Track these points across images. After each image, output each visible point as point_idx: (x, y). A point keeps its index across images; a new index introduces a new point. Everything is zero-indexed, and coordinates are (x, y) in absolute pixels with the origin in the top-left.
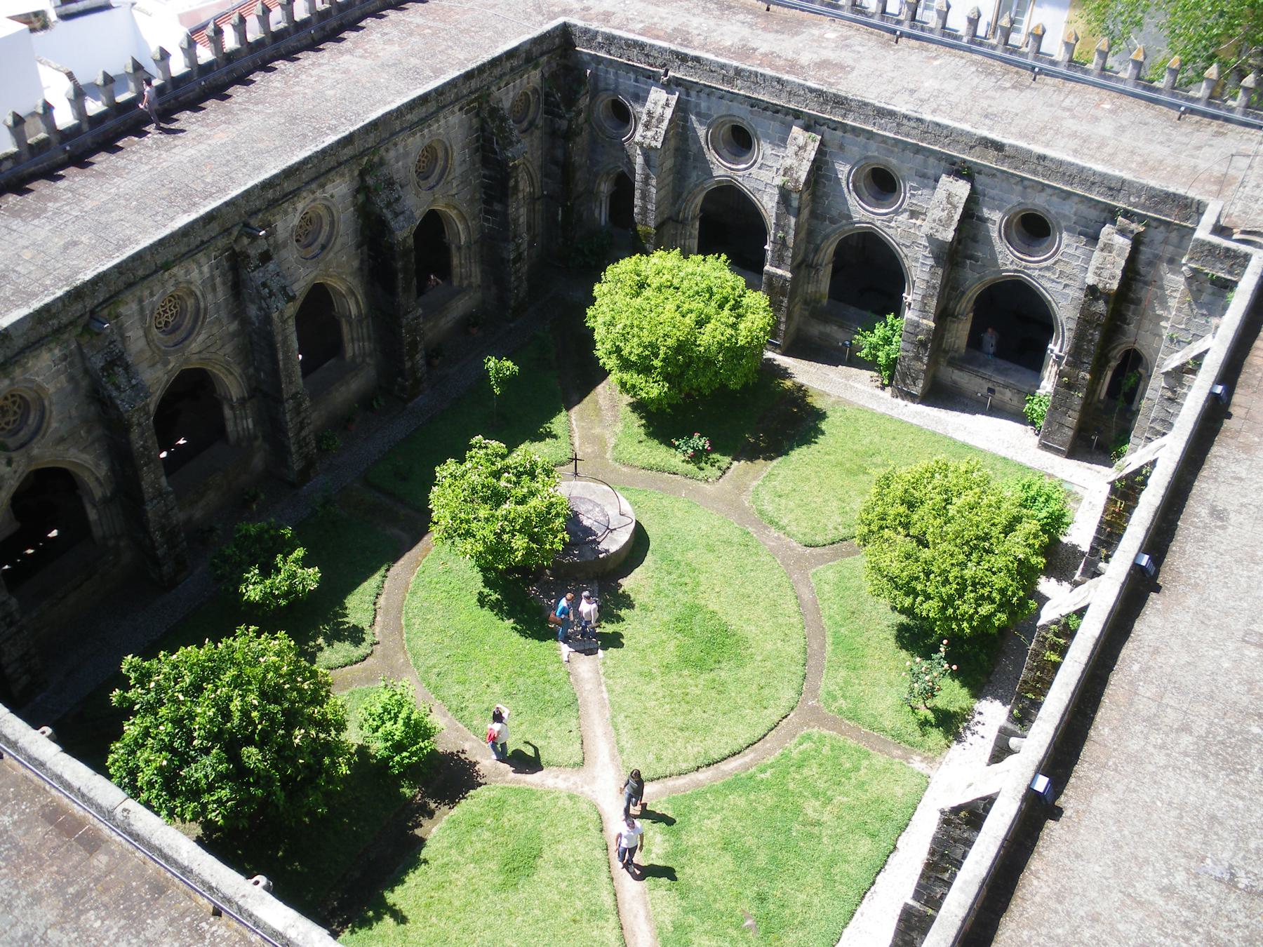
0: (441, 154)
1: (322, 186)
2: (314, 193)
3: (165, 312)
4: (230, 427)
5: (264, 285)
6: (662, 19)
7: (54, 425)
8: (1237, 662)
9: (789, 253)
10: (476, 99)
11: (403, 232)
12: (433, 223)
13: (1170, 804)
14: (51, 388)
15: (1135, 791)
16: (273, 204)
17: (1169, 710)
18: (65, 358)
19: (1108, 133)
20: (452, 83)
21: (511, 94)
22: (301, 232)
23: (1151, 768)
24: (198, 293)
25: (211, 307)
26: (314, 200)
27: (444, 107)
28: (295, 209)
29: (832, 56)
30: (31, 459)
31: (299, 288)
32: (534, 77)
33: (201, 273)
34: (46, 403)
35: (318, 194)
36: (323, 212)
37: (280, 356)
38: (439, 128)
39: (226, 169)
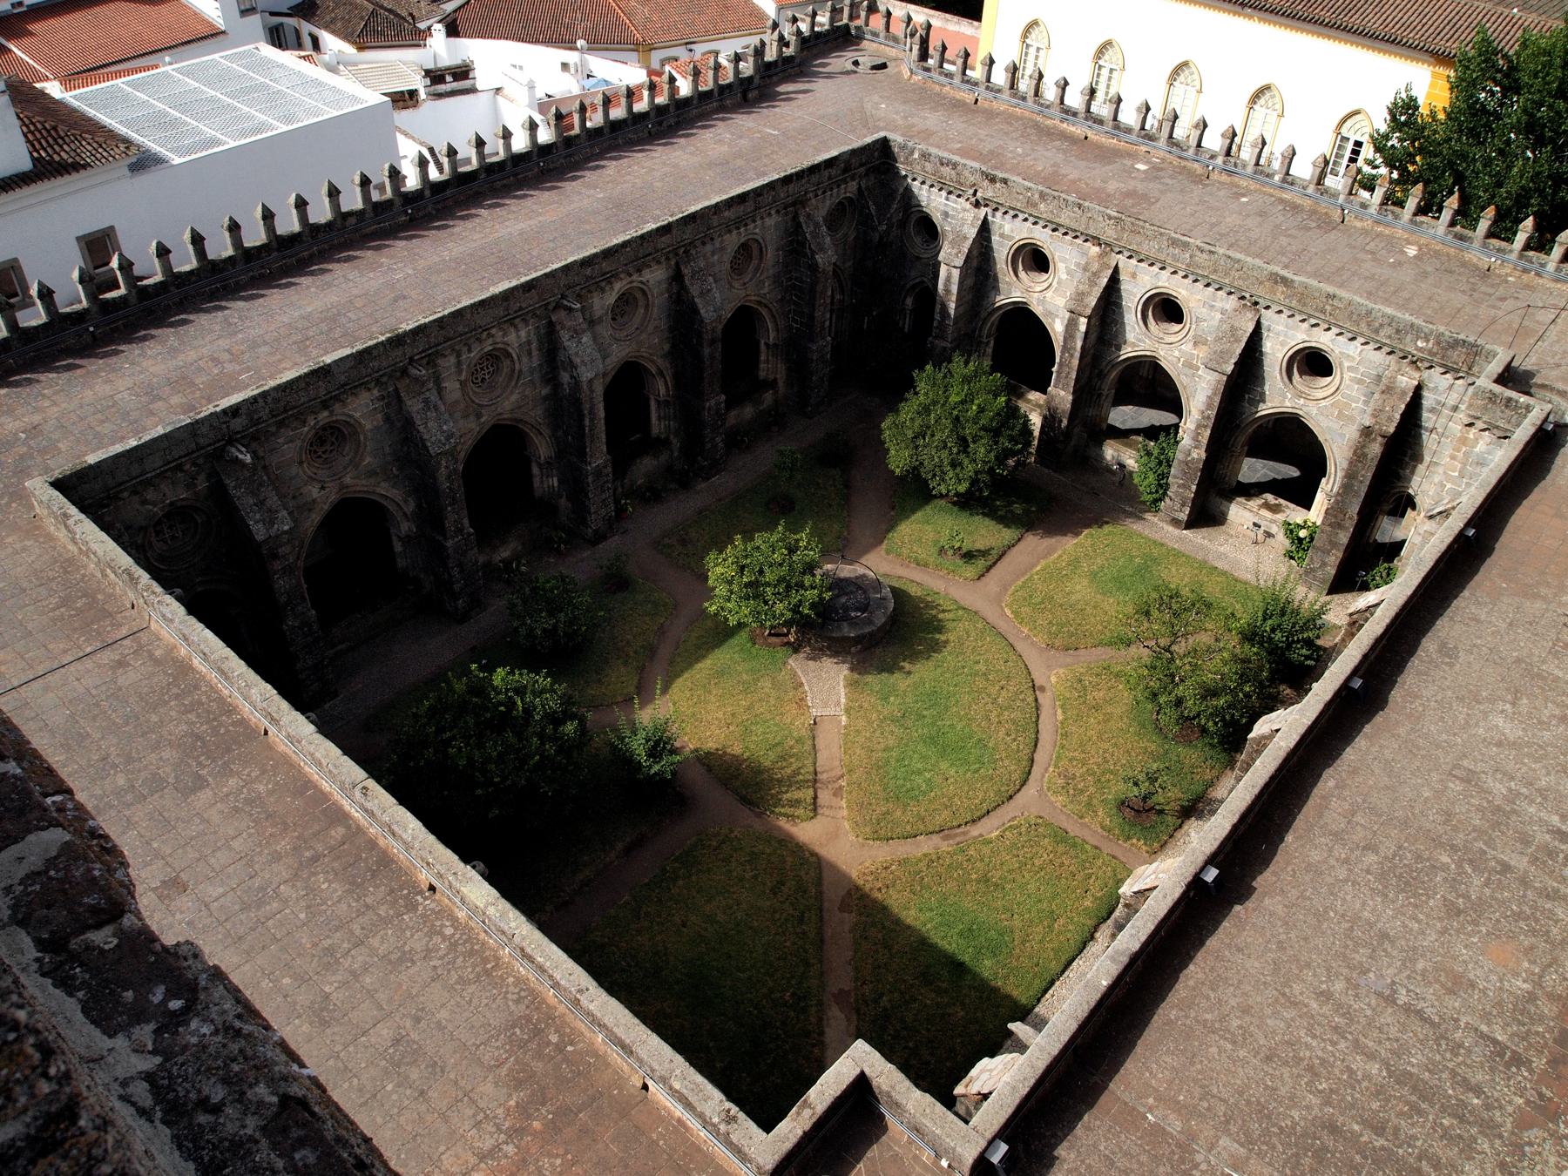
0: (755, 253)
1: (639, 271)
2: (630, 275)
3: (482, 369)
4: (536, 482)
6: (981, 140)
7: (368, 460)
8: (1439, 794)
12: (744, 320)
13: (1343, 916)
15: (1309, 899)
17: (1359, 828)
18: (382, 398)
20: (771, 186)
21: (828, 203)
22: (617, 311)
23: (1330, 880)
25: (525, 369)
28: (612, 288)
29: (1140, 187)
33: (518, 337)
35: (635, 277)
37: (587, 422)
38: (755, 227)
39: (551, 245)
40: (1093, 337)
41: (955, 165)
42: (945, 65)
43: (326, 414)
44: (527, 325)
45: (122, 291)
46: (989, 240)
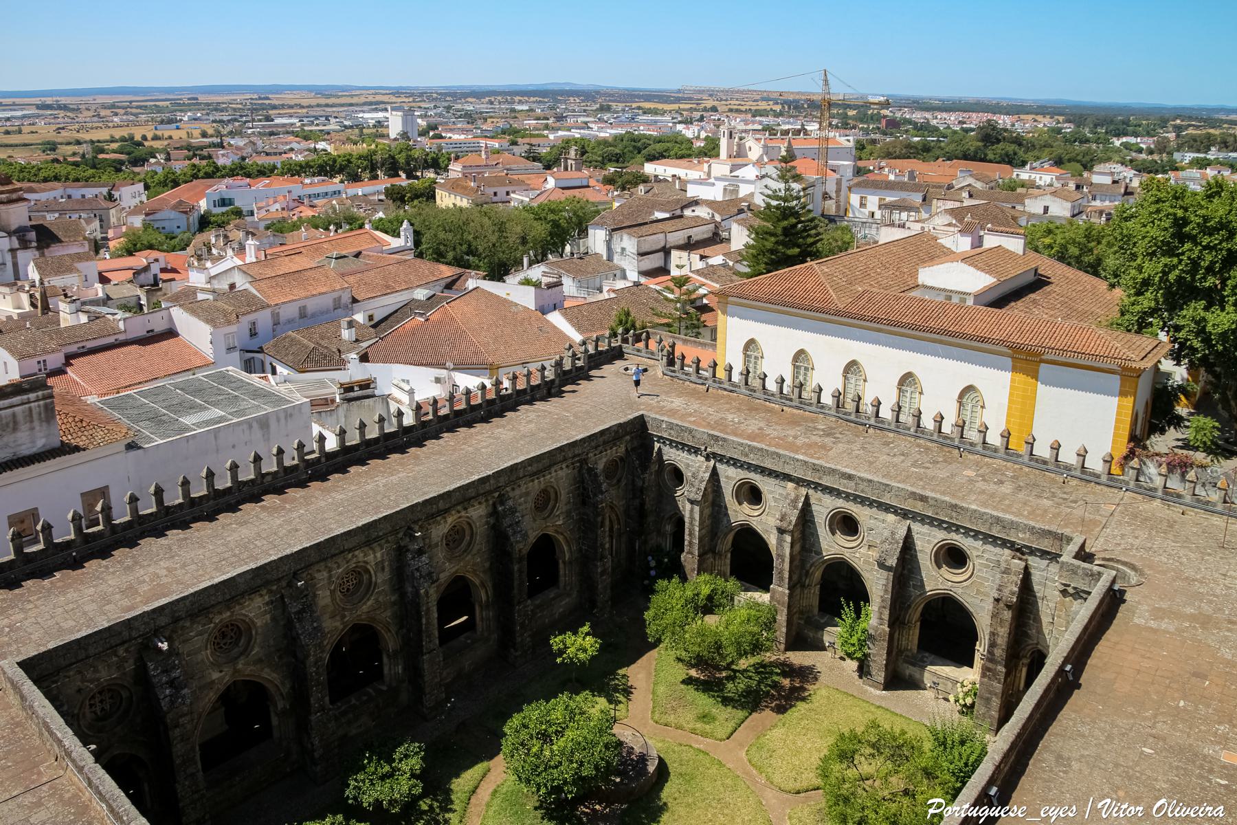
0: (553, 496)
1: (465, 509)
5: (417, 570)
7: (256, 650)
9: (786, 575)
10: (578, 461)
11: (521, 546)
12: (545, 545)
14: (259, 623)
16: (432, 516)
18: (272, 602)
19: (1008, 491)
21: (604, 460)
22: (450, 538)
24: (372, 572)
26: (460, 517)
27: (555, 464)
28: (446, 522)
30: (236, 671)
31: (444, 577)
32: (620, 450)
33: (375, 557)
34: (254, 632)
35: (463, 513)
36: (466, 527)
37: (424, 621)
40: (797, 547)
41: (691, 431)
42: (685, 368)
43: (228, 614)
44: (382, 549)
45: (101, 527)
46: (718, 481)
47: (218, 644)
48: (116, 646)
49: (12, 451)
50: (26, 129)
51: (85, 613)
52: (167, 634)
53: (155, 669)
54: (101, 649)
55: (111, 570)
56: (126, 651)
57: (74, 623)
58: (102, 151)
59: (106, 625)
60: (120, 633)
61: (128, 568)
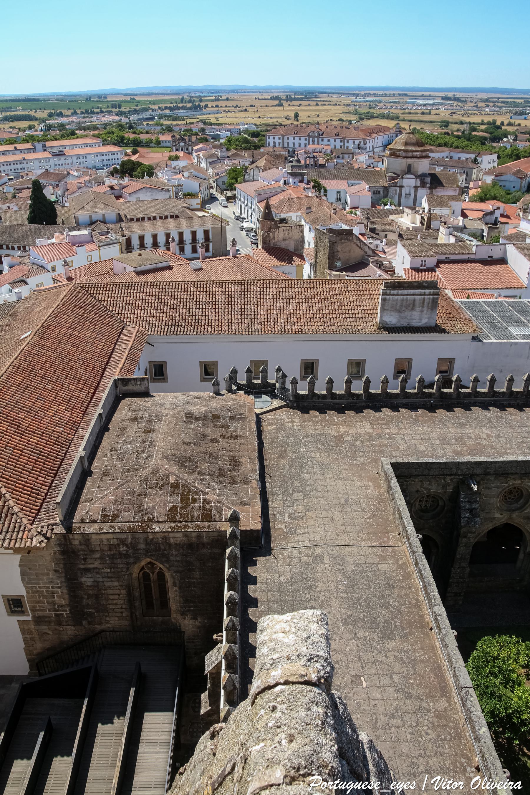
30: (510, 518)
43: (519, 482)
45: (451, 391)
47: (505, 496)
48: (447, 475)
49: (408, 321)
50: (433, 112)
51: (432, 444)
52: (478, 479)
53: (464, 498)
54: (437, 473)
55: (452, 421)
56: (451, 480)
57: (424, 449)
58: (475, 130)
59: (445, 461)
60: (451, 469)
61: (462, 425)
